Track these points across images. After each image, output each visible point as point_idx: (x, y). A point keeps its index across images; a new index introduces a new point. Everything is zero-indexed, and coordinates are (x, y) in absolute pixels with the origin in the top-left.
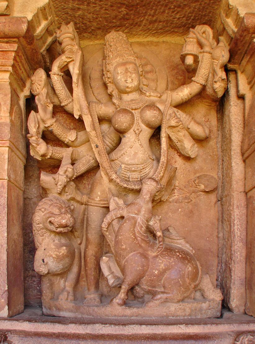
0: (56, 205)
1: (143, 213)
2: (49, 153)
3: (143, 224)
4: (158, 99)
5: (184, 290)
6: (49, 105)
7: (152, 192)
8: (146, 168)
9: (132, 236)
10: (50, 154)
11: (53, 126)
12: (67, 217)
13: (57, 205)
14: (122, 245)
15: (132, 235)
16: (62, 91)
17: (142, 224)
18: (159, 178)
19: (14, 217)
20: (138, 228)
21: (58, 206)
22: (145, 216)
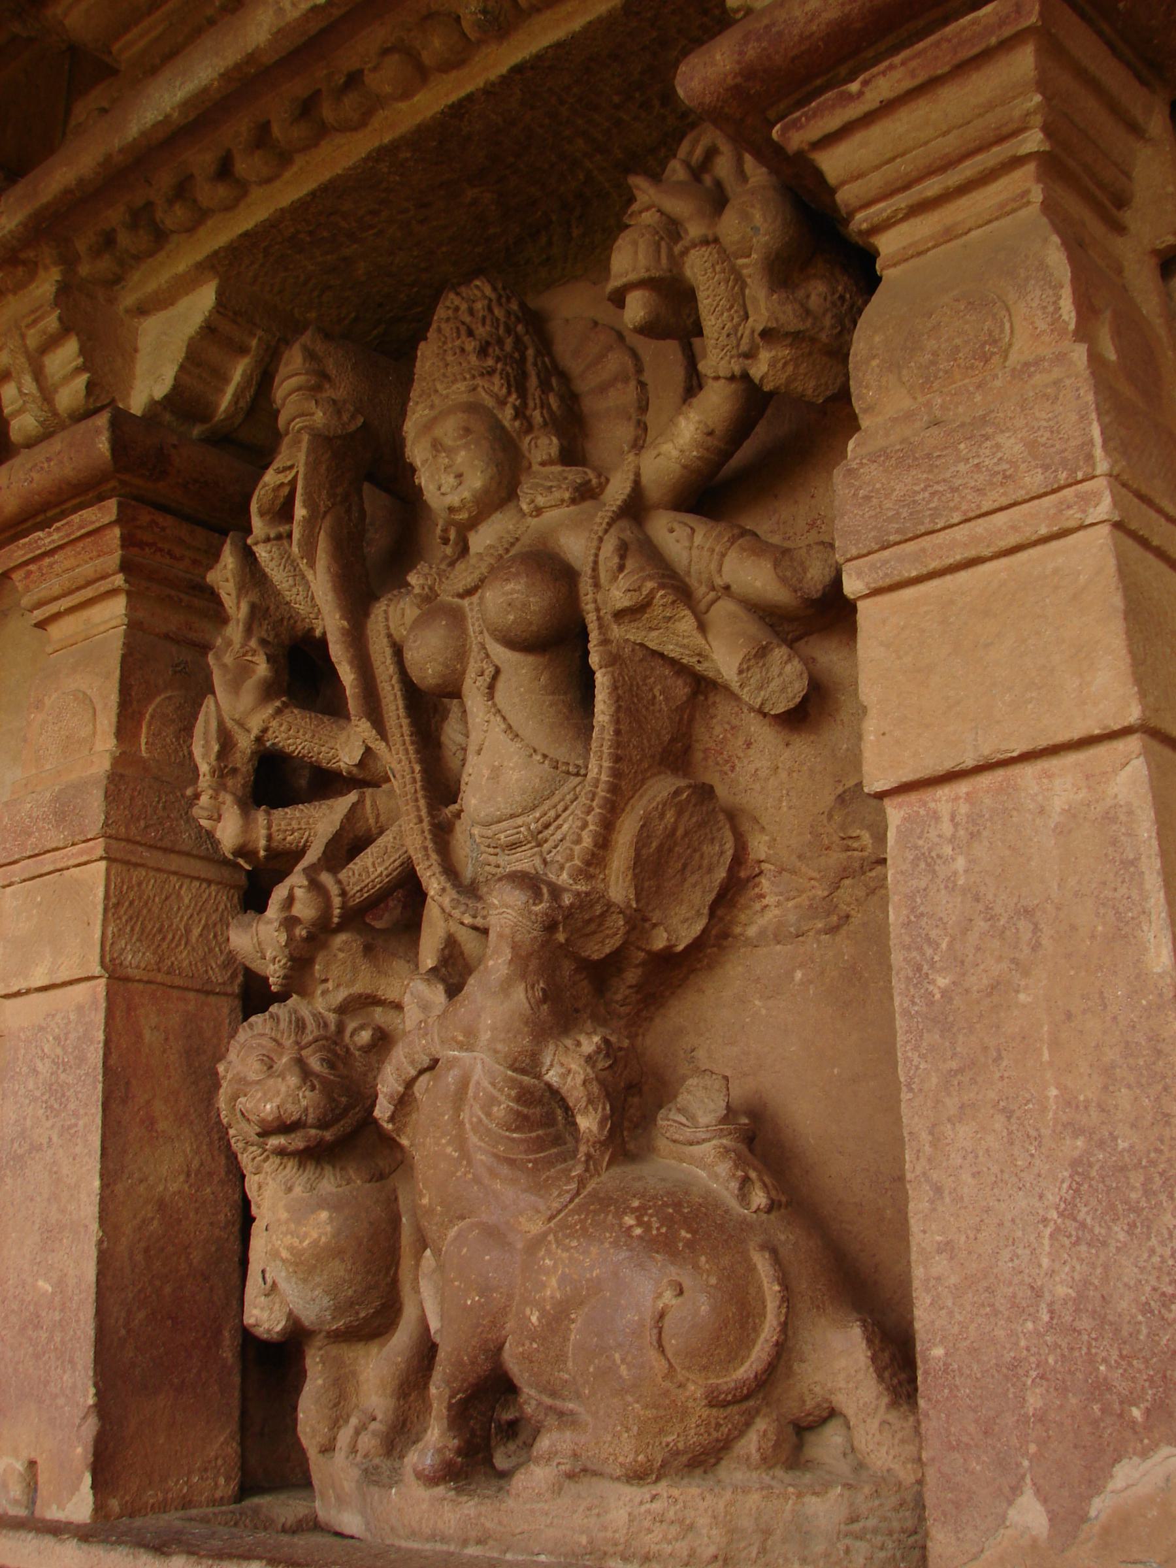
0: (254, 1042)
1: (485, 1036)
2: (257, 839)
3: (493, 1085)
4: (572, 508)
5: (650, 1413)
6: (254, 659)
7: (518, 938)
8: (560, 821)
9: (449, 1150)
10: (263, 843)
11: (270, 732)
12: (283, 1089)
13: (259, 1045)
14: (421, 1196)
15: (449, 1143)
16: (295, 590)
17: (490, 1088)
18: (577, 862)
19: (159, 1107)
20: (472, 1112)
21: (263, 1047)
22: (496, 1052)
